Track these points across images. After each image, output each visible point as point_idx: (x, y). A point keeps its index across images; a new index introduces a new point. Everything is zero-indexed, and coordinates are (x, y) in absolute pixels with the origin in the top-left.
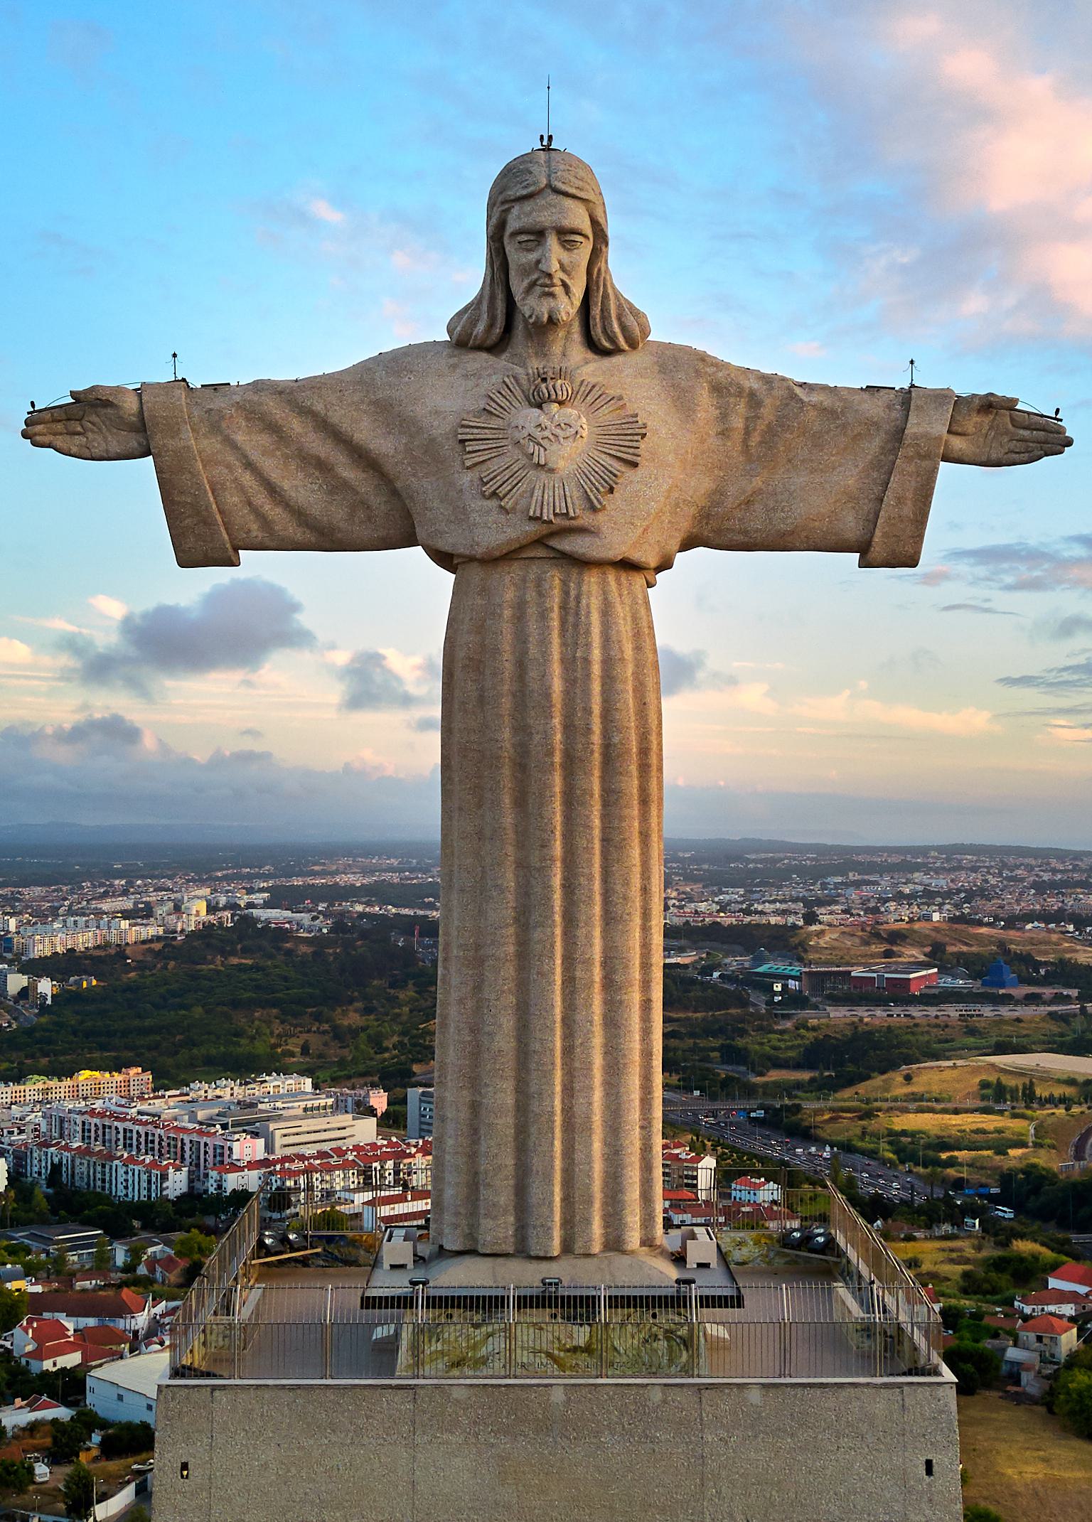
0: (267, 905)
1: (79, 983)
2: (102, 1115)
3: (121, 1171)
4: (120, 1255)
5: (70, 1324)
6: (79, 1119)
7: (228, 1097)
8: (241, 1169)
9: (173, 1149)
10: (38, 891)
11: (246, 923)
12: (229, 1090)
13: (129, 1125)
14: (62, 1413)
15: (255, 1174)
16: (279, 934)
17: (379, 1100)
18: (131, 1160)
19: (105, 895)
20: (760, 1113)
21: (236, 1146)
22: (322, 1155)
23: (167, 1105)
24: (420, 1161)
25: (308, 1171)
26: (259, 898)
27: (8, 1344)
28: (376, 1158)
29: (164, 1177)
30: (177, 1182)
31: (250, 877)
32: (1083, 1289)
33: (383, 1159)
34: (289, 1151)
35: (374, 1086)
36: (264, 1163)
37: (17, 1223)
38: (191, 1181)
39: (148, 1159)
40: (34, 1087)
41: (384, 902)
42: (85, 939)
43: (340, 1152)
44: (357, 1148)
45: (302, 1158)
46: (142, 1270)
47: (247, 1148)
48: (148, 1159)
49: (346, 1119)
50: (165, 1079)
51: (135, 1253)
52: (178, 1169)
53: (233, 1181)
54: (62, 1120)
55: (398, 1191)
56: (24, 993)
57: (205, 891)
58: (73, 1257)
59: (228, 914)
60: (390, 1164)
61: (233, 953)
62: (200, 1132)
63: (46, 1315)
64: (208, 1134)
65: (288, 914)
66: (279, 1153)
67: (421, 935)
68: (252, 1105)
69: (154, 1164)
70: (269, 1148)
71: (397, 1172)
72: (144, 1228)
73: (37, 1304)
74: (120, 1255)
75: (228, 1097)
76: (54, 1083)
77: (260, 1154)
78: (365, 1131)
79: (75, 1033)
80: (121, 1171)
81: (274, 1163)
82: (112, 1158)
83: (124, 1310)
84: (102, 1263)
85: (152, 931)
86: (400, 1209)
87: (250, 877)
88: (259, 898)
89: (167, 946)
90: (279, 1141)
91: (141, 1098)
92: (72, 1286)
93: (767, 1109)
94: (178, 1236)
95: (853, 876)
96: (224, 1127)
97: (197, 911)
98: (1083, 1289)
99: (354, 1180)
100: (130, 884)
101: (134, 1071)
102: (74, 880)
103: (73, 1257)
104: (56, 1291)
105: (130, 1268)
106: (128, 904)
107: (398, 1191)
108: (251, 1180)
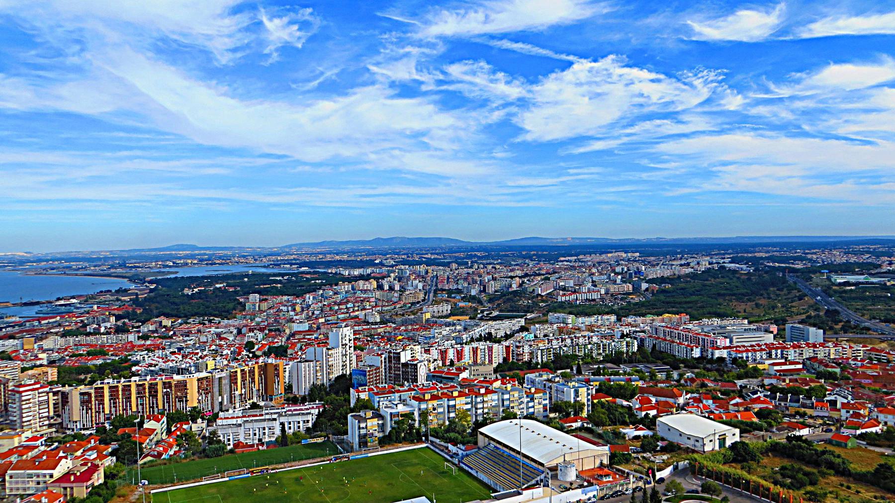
0: (730, 262)
1: (665, 286)
2: (670, 328)
3: (677, 347)
4: (675, 375)
5: (653, 400)
6: (662, 329)
7: (716, 324)
8: (721, 349)
9: (695, 340)
10: (653, 258)
12: (716, 321)
13: (680, 332)
14: (650, 433)
15: (725, 351)
16: (734, 272)
17: (774, 328)
18: (680, 343)
19: (674, 259)
22: (752, 346)
23: (693, 326)
24: (792, 351)
25: (747, 351)
26: (727, 260)
27: (631, 404)
28: (773, 348)
29: (692, 350)
30: (697, 353)
31: (724, 254)
33: (777, 348)
34: (739, 344)
35: (772, 323)
36: (729, 347)
37: (639, 362)
38: (702, 352)
39: (686, 343)
40: (649, 318)
41: (774, 262)
42: (667, 273)
43: (759, 345)
44: (766, 344)
45: (744, 346)
46: (682, 382)
47: (722, 342)
48: (686, 343)
49: (761, 334)
50: (693, 318)
51: (681, 376)
52: (697, 347)
53: (717, 354)
55: (783, 361)
56: (647, 290)
57: (708, 258)
58: (659, 376)
59: (716, 265)
60: (779, 351)
61: (718, 278)
62: (705, 335)
63: (645, 395)
64: (708, 336)
65: (737, 265)
66: (735, 344)
67: (789, 272)
68: (725, 327)
69: (688, 345)
70: (731, 342)
71: (782, 354)
72: (685, 367)
73: (642, 390)
74: (675, 375)
75: (716, 324)
76: (655, 317)
77: (728, 344)
78: (769, 338)
79: (663, 302)
80: (677, 347)
81: (733, 347)
82: (673, 342)
83: (675, 397)
84: (669, 377)
85: (689, 270)
87: (724, 254)
88: (727, 260)
90: (735, 340)
91: (685, 323)
92: (657, 386)
94: (696, 370)
96: (714, 334)
97: (704, 264)
100: (683, 256)
101: (682, 315)
102: (665, 255)
103: (659, 376)
104: (651, 386)
105: (679, 381)
106: (683, 262)
107: (783, 361)
108: (724, 354)
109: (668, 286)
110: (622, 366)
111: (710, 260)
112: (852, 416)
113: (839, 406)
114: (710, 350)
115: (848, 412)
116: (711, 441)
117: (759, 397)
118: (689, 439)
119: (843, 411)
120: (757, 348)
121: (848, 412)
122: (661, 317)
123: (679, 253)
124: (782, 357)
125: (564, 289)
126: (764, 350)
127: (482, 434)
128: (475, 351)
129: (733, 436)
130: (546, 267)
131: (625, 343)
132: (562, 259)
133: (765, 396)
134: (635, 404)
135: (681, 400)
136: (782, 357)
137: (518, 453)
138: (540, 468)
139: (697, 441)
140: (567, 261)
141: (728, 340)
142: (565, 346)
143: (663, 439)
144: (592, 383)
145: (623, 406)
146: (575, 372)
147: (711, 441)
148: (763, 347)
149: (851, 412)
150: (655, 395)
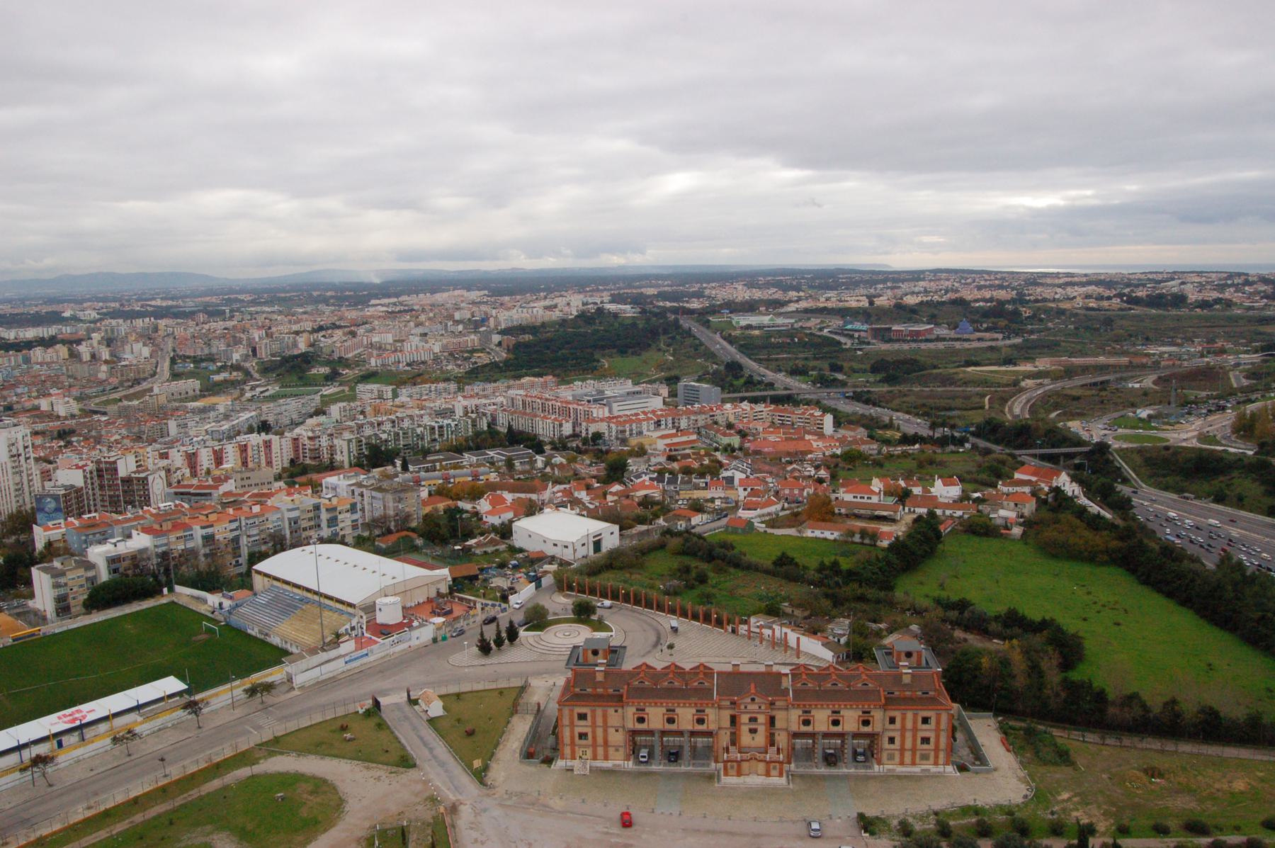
11: (600, 311)
18: (545, 417)
20: (851, 394)
21: (595, 411)
22: (637, 414)
29: (561, 425)
30: (567, 429)
32: (1034, 479)
38: (574, 427)
39: (553, 417)
43: (644, 413)
47: (599, 412)
48: (553, 417)
54: (512, 399)
55: (674, 431)
63: (499, 492)
69: (555, 419)
70: (610, 411)
71: (673, 423)
76: (511, 382)
77: (607, 414)
82: (536, 416)
86: (676, 440)
89: (563, 323)
93: (854, 392)
95: (889, 284)
98: (1034, 479)
99: (652, 428)
108: (602, 428)
109: (527, 337)
110: (466, 455)
111: (585, 300)
112: (749, 495)
113: (736, 482)
114: (584, 424)
115: (745, 490)
116: (583, 545)
117: (644, 481)
118: (555, 545)
119: (741, 489)
120: (642, 416)
121: (745, 490)
122: (517, 382)
123: (543, 290)
124: (673, 427)
125: (380, 348)
126: (652, 419)
127: (259, 572)
128: (243, 449)
129: (611, 537)
130: (352, 314)
131: (470, 421)
132: (373, 302)
133: (651, 479)
134: (484, 505)
135: (546, 495)
136: (673, 427)
137: (316, 593)
138: (350, 610)
139: (566, 547)
140: (382, 305)
141: (606, 409)
142: (384, 432)
143: (521, 550)
144: (423, 483)
145: (467, 512)
146: (399, 469)
147: (583, 545)
148: (650, 415)
149: (749, 490)
150: (512, 490)
